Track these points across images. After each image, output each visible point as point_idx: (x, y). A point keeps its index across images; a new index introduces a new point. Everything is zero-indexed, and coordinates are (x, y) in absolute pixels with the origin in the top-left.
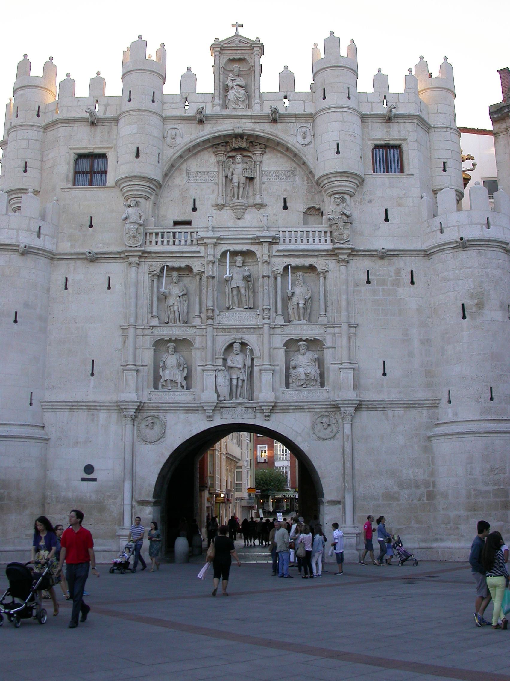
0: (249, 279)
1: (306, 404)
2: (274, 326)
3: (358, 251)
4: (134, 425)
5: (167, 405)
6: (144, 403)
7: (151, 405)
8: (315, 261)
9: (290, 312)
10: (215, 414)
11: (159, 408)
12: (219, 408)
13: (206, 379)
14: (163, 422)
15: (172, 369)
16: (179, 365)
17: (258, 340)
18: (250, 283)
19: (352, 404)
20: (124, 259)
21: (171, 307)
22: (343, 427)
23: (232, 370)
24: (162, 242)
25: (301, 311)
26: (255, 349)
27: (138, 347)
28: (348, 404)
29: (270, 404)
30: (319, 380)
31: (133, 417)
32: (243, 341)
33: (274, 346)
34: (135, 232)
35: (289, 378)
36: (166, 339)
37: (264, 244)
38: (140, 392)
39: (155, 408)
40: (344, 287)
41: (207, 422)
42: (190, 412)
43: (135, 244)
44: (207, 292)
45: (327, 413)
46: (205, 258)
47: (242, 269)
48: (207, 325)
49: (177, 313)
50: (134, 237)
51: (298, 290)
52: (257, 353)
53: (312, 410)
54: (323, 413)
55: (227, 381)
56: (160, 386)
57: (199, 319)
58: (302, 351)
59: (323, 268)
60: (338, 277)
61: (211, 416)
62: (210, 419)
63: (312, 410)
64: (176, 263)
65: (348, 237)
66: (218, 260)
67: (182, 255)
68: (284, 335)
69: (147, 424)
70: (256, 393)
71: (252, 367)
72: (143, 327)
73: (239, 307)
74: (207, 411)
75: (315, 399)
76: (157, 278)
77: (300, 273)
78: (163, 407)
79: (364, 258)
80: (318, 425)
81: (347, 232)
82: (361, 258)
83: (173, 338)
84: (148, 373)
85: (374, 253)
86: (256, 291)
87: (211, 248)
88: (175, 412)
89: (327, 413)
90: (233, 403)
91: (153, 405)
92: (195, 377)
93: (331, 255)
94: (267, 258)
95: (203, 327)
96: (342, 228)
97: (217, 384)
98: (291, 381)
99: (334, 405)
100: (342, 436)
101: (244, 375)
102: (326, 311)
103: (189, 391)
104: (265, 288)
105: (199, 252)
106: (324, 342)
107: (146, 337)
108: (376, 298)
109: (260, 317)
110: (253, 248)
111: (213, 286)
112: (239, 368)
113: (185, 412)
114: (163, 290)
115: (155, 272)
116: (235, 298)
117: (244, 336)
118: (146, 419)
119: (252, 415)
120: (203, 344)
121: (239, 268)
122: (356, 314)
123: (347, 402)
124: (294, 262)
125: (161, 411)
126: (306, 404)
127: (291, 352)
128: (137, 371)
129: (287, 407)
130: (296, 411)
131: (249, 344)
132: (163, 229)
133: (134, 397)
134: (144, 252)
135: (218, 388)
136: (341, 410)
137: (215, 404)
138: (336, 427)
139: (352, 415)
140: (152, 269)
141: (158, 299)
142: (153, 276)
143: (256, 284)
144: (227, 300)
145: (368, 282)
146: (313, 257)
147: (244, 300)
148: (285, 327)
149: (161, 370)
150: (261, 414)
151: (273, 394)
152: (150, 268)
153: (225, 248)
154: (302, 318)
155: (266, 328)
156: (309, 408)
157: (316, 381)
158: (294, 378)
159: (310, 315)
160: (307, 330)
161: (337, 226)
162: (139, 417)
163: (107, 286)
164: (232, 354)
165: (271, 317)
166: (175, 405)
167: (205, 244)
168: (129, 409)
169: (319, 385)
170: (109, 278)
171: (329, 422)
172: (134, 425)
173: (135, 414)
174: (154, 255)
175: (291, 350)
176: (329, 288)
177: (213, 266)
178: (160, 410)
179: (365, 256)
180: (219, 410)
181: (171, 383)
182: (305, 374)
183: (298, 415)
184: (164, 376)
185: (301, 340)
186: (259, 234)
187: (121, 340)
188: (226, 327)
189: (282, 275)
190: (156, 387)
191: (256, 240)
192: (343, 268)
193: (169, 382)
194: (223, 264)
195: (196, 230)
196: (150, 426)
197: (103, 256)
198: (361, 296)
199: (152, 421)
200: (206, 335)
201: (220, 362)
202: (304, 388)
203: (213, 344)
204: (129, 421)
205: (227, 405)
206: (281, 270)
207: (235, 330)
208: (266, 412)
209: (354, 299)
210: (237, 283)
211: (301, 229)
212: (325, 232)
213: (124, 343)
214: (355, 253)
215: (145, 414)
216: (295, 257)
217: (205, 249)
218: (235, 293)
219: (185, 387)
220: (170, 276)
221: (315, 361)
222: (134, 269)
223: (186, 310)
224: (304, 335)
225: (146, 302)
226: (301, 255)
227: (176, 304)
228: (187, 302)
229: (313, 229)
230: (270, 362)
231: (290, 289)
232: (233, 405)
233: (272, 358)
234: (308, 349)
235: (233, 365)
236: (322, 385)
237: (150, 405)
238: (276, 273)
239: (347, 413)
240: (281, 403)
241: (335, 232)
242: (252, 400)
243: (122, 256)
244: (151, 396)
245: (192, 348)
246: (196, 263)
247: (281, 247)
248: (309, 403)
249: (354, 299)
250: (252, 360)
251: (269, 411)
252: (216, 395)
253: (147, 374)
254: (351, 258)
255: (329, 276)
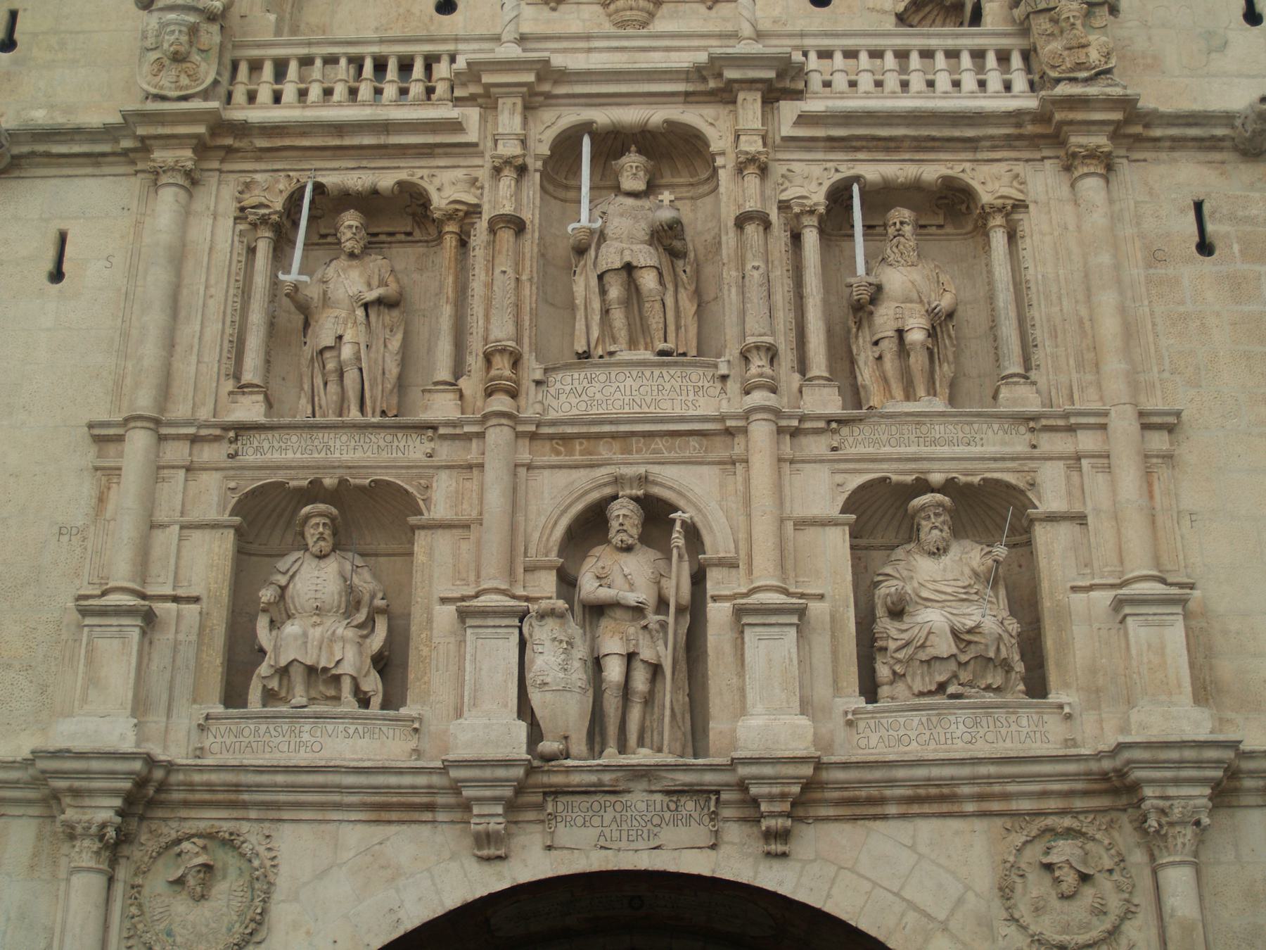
0: (677, 244)
1: (966, 771)
2: (795, 423)
3: (1150, 119)
4: (111, 880)
5: (280, 779)
6: (170, 767)
7: (205, 777)
8: (967, 165)
9: (866, 374)
10: (514, 828)
11: (246, 797)
12: (539, 798)
13: (474, 656)
14: (256, 863)
15: (315, 619)
16: (352, 601)
17: (722, 486)
18: (680, 263)
19: (1199, 764)
20: (133, 163)
21: (327, 355)
22: (1157, 887)
23: (606, 624)
24: (303, 94)
25: (918, 361)
26: (711, 530)
27: (161, 516)
28: (1180, 764)
29: (790, 770)
30: (1019, 667)
31: (111, 833)
32: (656, 490)
33: (800, 512)
34: (184, 38)
35: (872, 660)
36: (293, 484)
37: (741, 96)
38: (156, 721)
39: (220, 797)
40: (1105, 259)
41: (474, 867)
42: (394, 816)
43: (181, 88)
44: (489, 285)
45: (1067, 822)
46: (481, 155)
47: (646, 203)
48: (486, 417)
49: (351, 376)
50: (178, 58)
51: (896, 279)
52: (718, 543)
53: (996, 806)
54: (1050, 821)
55: (577, 664)
56: (255, 694)
57: (451, 396)
58: (932, 533)
59: (1005, 191)
60: (1072, 227)
61: (498, 832)
62: (492, 852)
63: (996, 806)
64: (355, 174)
65: (1107, 56)
66: (539, 164)
67: (382, 140)
68: (843, 466)
69: (180, 873)
70: (718, 726)
71: (695, 610)
72: (192, 430)
73: (632, 344)
74: (476, 810)
75: (1008, 747)
76: (269, 234)
77: (902, 214)
78: (259, 788)
79: (1176, 155)
80: (1031, 877)
81: (1095, 39)
82: (1163, 155)
83: (328, 482)
84: (200, 633)
85: (1219, 132)
86: (709, 294)
87: (513, 113)
88: (319, 816)
89: (1067, 822)
90: (606, 768)
91: (214, 777)
92: (425, 651)
93: (1033, 141)
94: (752, 145)
95: (467, 429)
96: (1078, 22)
97: (529, 676)
98: (883, 672)
99: (1104, 777)
100: (1154, 932)
101: (661, 642)
102: (1028, 368)
103: (392, 713)
104: (749, 267)
105: (456, 126)
106: (1030, 495)
107: (205, 476)
108: (1246, 308)
109: (733, 386)
110: (693, 116)
111: (517, 264)
112: (638, 610)
113: (373, 816)
114: (292, 276)
115: (266, 211)
116: (618, 317)
117: (655, 469)
118: (177, 849)
119: (700, 833)
120: (465, 506)
121: (630, 201)
122: (1166, 375)
123: (1174, 754)
124: (874, 170)
125: (253, 814)
126: (966, 771)
127: (874, 554)
128: (149, 619)
129: (874, 792)
130: (916, 809)
131: (681, 503)
132: (310, 44)
133: (122, 737)
134: (220, 126)
135: (535, 697)
136: (1143, 799)
137: (519, 772)
138: (1120, 889)
139: (1197, 823)
140: (250, 200)
141: (272, 326)
142: (254, 226)
143: (708, 270)
144: (580, 325)
145: (1205, 247)
146: (954, 150)
147: (655, 322)
148: (845, 431)
149: (262, 623)
150: (746, 829)
151: (804, 721)
152: (246, 196)
153: (570, 117)
154: (921, 391)
155: (761, 432)
156: (981, 797)
157: (1006, 666)
158: (900, 655)
159: (953, 385)
160: (950, 443)
161: (1055, 21)
162: (143, 838)
163: (49, 265)
164: (597, 550)
165: (783, 387)
166: (319, 779)
167: (487, 101)
168: (91, 793)
169: (1022, 687)
170: (63, 238)
171: (1085, 863)
172: (111, 880)
173: (119, 819)
174: (261, 143)
175: (872, 541)
176: (1032, 273)
177: (517, 181)
178: (245, 805)
179: (1177, 144)
180: (540, 807)
181: (309, 685)
182: (955, 634)
183: (926, 829)
184: (276, 648)
185: (922, 486)
186: (718, 47)
187: (87, 489)
188: (575, 430)
189: (821, 217)
190: (234, 696)
191: (704, 79)
192: (1092, 187)
193: (297, 676)
194: (562, 194)
195: (451, 47)
196: (191, 881)
197: (41, 148)
198: (1182, 303)
199: (202, 859)
200: (481, 466)
201: (546, 584)
202: (952, 696)
203: (514, 504)
204: (85, 854)
205: (576, 779)
206: (818, 197)
207: (616, 445)
208: (772, 815)
209: (1152, 313)
210: (627, 252)
211: (900, 42)
212: (1003, 58)
213: (101, 500)
214: (1138, 129)
215: (174, 825)
216: (877, 149)
217: (483, 119)
218: (614, 292)
219: (376, 701)
220: (330, 239)
221: (995, 583)
222: (168, 198)
223: (393, 369)
224: (936, 465)
225: (213, 329)
226: (905, 137)
227: (347, 338)
228: (399, 336)
229: (950, 43)
230: (784, 580)
231: (861, 269)
232: (607, 778)
233: (789, 564)
234: (958, 532)
235: (604, 594)
236: (1037, 687)
237: (197, 778)
238: (797, 210)
239: (1176, 813)
240: (846, 765)
241: (1048, 42)
242: (696, 756)
243: (126, 144)
244: (208, 741)
245: (413, 520)
246: (446, 176)
247: (813, 105)
248: (983, 770)
249: (1152, 313)
250: (698, 579)
251: (786, 807)
252: (522, 728)
253: (194, 638)
254: (1123, 152)
255: (1032, 223)
